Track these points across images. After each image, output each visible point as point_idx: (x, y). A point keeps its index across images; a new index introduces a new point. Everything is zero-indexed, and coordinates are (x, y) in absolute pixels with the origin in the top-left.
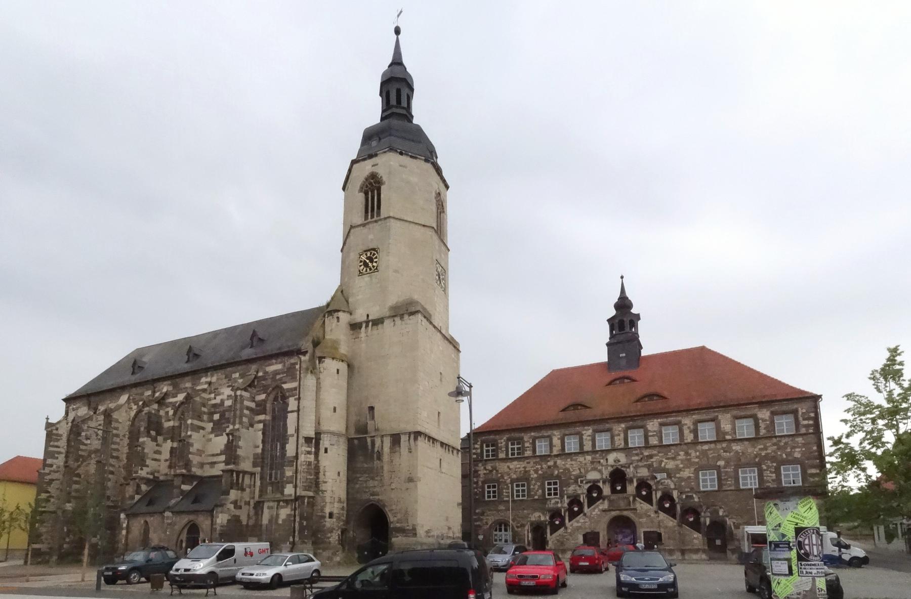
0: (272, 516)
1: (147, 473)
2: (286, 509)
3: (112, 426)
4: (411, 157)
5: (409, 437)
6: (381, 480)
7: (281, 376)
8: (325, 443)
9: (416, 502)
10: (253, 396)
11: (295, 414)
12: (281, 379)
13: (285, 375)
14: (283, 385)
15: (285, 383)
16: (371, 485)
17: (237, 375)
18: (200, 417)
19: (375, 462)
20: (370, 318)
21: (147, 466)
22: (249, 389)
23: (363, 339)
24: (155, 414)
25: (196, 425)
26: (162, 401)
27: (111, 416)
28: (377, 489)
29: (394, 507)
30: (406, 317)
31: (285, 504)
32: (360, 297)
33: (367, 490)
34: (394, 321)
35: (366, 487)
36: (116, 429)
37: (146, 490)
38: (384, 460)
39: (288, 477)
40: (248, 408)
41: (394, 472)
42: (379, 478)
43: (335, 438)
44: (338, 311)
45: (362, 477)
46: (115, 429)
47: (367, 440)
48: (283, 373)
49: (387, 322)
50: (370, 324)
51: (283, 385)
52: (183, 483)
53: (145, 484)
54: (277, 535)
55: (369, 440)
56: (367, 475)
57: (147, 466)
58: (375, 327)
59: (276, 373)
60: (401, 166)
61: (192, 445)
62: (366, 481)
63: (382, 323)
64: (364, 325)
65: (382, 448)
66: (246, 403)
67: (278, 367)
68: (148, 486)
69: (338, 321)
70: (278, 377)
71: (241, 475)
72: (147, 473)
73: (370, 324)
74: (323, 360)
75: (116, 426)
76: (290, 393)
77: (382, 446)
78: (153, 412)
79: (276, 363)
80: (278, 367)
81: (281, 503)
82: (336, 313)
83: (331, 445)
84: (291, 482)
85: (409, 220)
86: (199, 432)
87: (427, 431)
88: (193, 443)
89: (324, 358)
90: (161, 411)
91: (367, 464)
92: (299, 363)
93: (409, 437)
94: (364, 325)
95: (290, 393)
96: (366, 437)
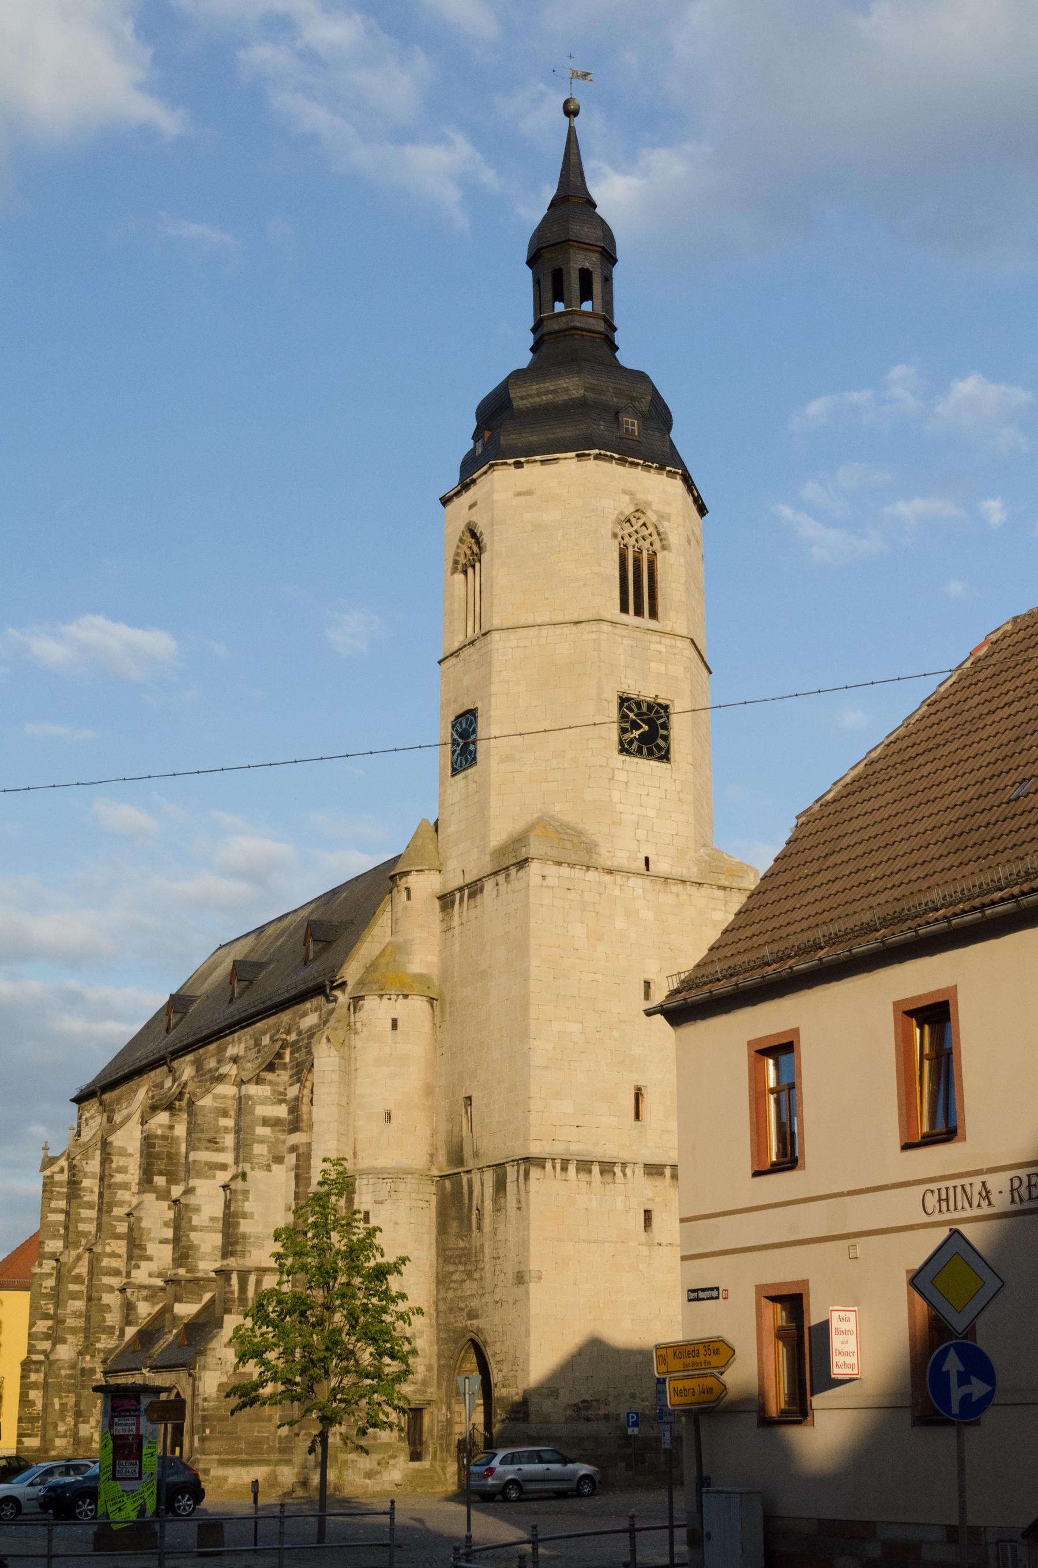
1: (150, 1275)
3: (114, 1165)
4: (543, 462)
5: (518, 1171)
6: (481, 1279)
8: (364, 1199)
9: (527, 1334)
10: (281, 1089)
16: (468, 1293)
18: (216, 1143)
19: (474, 1235)
21: (150, 1259)
22: (269, 1076)
24: (164, 1137)
25: (206, 1163)
26: (177, 1103)
27: (110, 1143)
28: (475, 1303)
29: (497, 1347)
30: (513, 871)
33: (463, 1305)
34: (497, 884)
35: (461, 1298)
36: (123, 1170)
37: (149, 1314)
38: (485, 1231)
40: (266, 1122)
41: (499, 1258)
42: (476, 1276)
43: (385, 1187)
44: (407, 873)
45: (457, 1271)
46: (120, 1172)
47: (461, 1179)
49: (489, 885)
52: (178, 1299)
53: (145, 1299)
55: (465, 1178)
56: (463, 1269)
57: (150, 1259)
58: (472, 901)
60: (519, 494)
61: (197, 1210)
62: (463, 1281)
63: (482, 890)
64: (458, 896)
65: (482, 1202)
66: (262, 1111)
68: (154, 1304)
69: (409, 898)
71: (252, 1278)
72: (150, 1275)
73: (466, 892)
74: (361, 1002)
75: (121, 1164)
77: (483, 1195)
78: (159, 1132)
82: (404, 880)
83: (376, 1202)
85: (539, 621)
86: (214, 1177)
87: (574, 1148)
88: (199, 1205)
89: (362, 998)
90: (176, 1126)
91: (463, 1240)
93: (518, 1171)
96: (459, 1173)
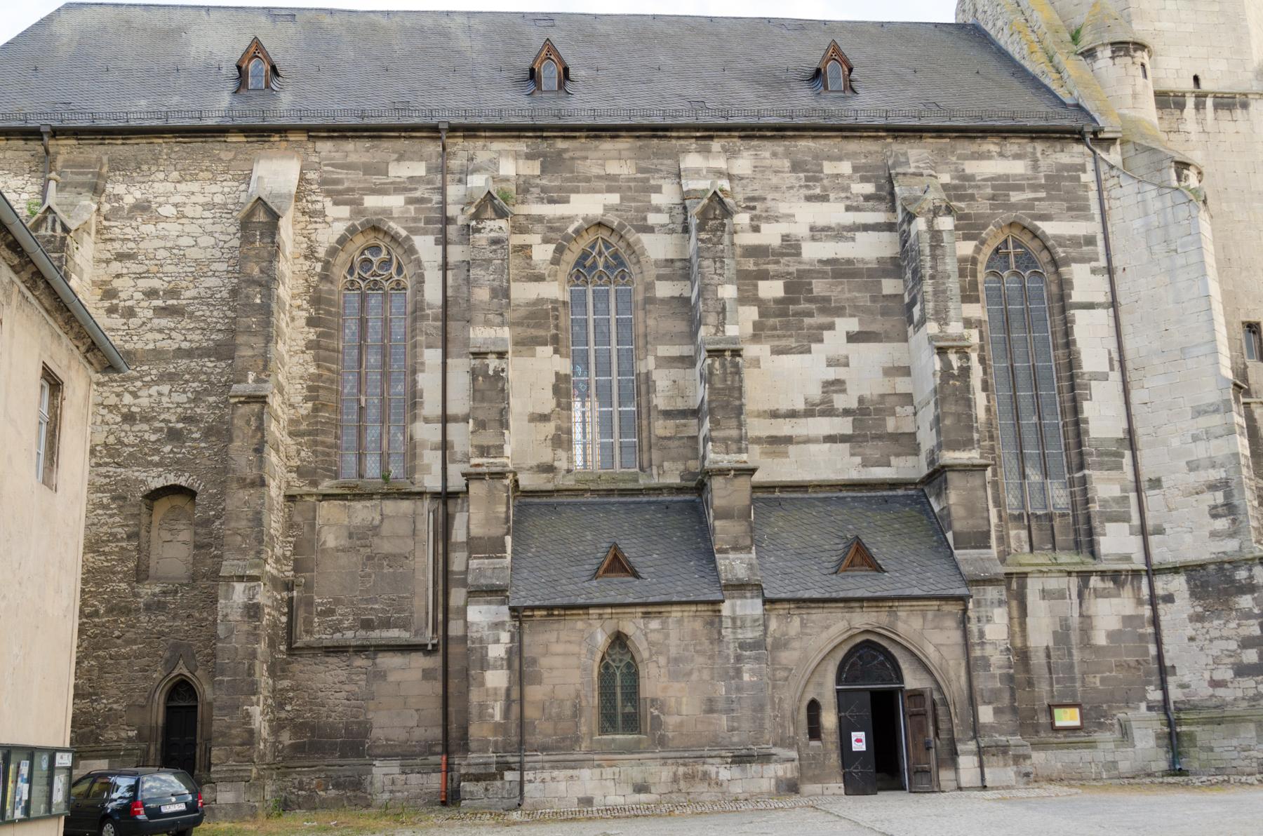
0: (1065, 624)
2: (1114, 601)
7: (1031, 195)
11: (1103, 317)
12: (1029, 204)
13: (1043, 194)
14: (1039, 224)
15: (1046, 217)
17: (845, 168)
20: (1205, 86)
23: (1193, 137)
31: (1111, 585)
32: (1165, 25)
39: (1104, 503)
48: (1035, 188)
50: (1209, 102)
51: (1039, 224)
54: (1096, 681)
58: (1223, 114)
59: (1003, 185)
63: (1245, 106)
64: (1190, 102)
67: (1018, 168)
70: (1015, 197)
76: (1073, 252)
79: (1001, 155)
80: (1018, 168)
81: (1095, 582)
84: (1123, 518)
92: (1090, 166)
94: (1190, 102)
95: (1073, 252)
